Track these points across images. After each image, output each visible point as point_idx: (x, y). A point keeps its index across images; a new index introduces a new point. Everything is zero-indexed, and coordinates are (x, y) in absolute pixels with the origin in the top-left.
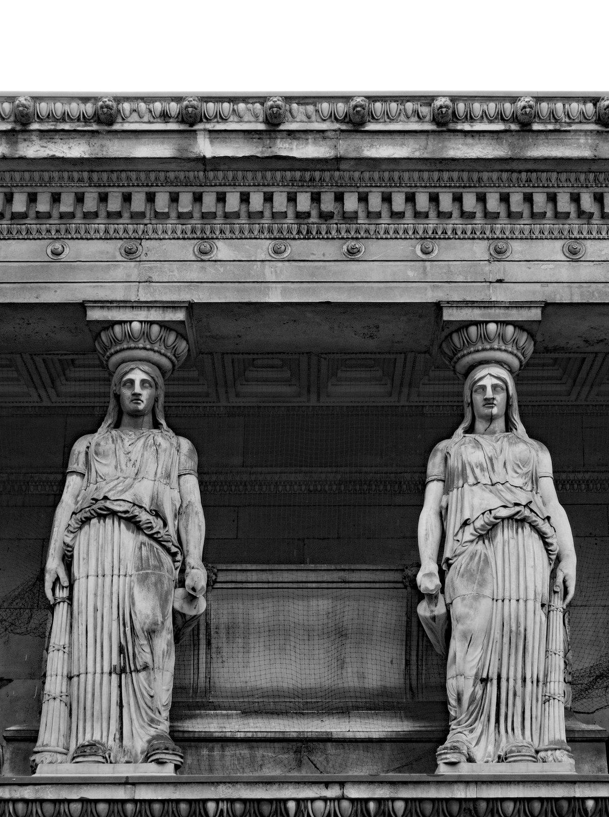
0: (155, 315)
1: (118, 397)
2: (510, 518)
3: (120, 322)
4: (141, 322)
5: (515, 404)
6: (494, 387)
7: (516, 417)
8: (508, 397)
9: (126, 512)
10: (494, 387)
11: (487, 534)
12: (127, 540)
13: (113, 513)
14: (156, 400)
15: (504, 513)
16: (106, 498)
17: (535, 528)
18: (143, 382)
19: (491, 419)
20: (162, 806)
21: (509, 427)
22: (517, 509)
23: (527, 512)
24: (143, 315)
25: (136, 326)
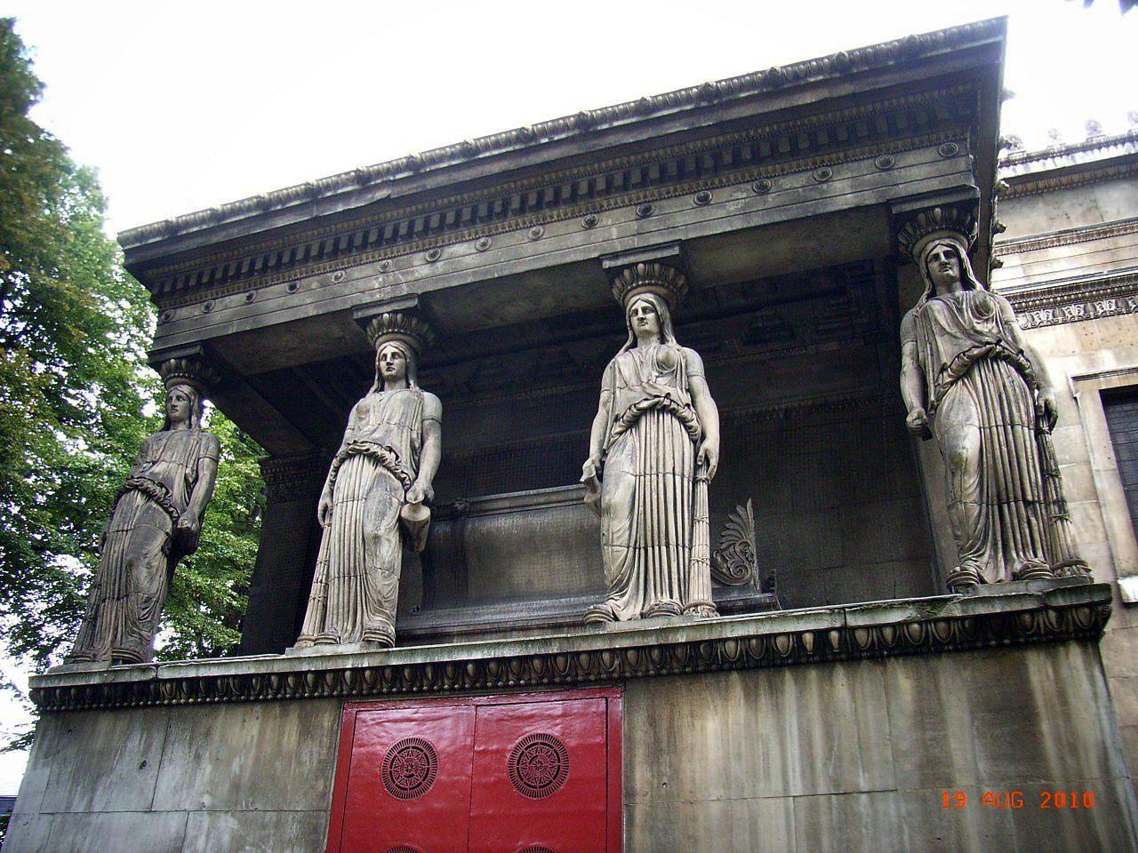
0: (395, 307)
1: (379, 369)
2: (651, 409)
3: (375, 316)
4: (388, 313)
5: (668, 322)
6: (644, 310)
8: (658, 317)
9: (368, 450)
10: (644, 310)
11: (634, 423)
12: (369, 470)
13: (359, 452)
14: (407, 368)
15: (645, 404)
16: (355, 442)
17: (673, 412)
18: (394, 355)
19: (648, 333)
20: (759, 641)
21: (663, 340)
22: (657, 400)
23: (667, 402)
24: (389, 308)
25: (386, 316)
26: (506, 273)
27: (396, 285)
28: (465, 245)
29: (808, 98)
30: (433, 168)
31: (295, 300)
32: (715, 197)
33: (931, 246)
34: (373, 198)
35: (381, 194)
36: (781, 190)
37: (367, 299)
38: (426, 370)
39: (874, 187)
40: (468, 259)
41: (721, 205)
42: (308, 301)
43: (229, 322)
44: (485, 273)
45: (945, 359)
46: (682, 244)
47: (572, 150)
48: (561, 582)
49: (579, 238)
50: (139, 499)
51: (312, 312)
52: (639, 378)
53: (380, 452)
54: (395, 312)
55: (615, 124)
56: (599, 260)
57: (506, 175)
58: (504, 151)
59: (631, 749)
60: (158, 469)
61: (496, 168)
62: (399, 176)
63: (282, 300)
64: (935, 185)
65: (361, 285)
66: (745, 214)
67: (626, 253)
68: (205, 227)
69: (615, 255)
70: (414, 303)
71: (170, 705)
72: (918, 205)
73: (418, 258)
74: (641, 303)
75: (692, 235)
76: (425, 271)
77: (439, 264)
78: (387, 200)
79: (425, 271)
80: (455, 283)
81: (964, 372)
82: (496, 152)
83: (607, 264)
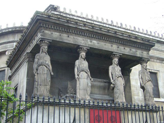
1: (81, 56)
3: (83, 48)
7: (118, 64)
11: (118, 77)
12: (86, 74)
13: (84, 71)
15: (120, 76)
26: (101, 49)
27: (86, 44)
28: (95, 41)
29: (139, 41)
30: (95, 28)
31: (69, 39)
32: (126, 48)
33: (144, 64)
34: (86, 28)
35: (87, 28)
36: (132, 51)
37: (82, 45)
38: (87, 58)
39: (141, 55)
40: (96, 44)
41: (126, 50)
42: (72, 40)
43: (57, 38)
44: (99, 48)
45: (147, 79)
46: (123, 54)
47: (113, 35)
48: (96, 92)
49: (110, 47)
50: (45, 68)
51: (73, 43)
52: (118, 71)
53: (87, 72)
54: (86, 49)
55: (119, 34)
56: (113, 52)
57: (104, 34)
58: (105, 30)
59: (122, 118)
60: (47, 62)
61: (104, 33)
62: (90, 27)
63: (67, 38)
64: (146, 57)
65: (80, 41)
66: (129, 52)
67: (117, 53)
68: (55, 19)
69: (115, 52)
70: (89, 48)
71: (63, 106)
72: (145, 59)
73: (89, 40)
74: (116, 60)
75: (123, 53)
76: (90, 43)
77: (92, 43)
78: (87, 30)
79: (90, 43)
80: (95, 48)
81: (148, 82)
82: (104, 30)
83: (114, 53)
